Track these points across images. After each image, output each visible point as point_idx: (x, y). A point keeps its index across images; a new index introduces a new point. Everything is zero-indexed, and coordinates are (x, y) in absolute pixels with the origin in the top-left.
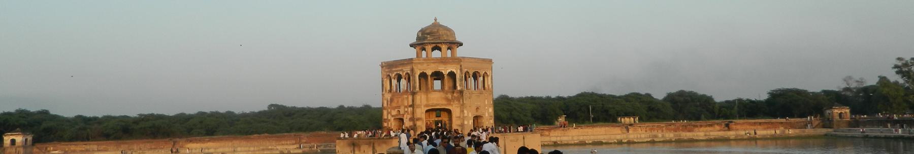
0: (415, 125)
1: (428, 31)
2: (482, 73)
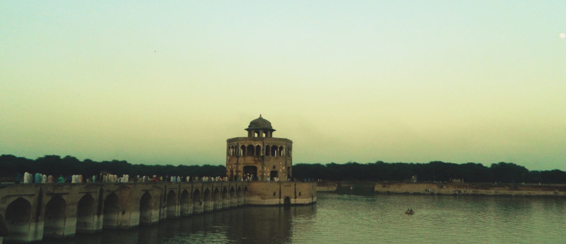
0: (237, 174)
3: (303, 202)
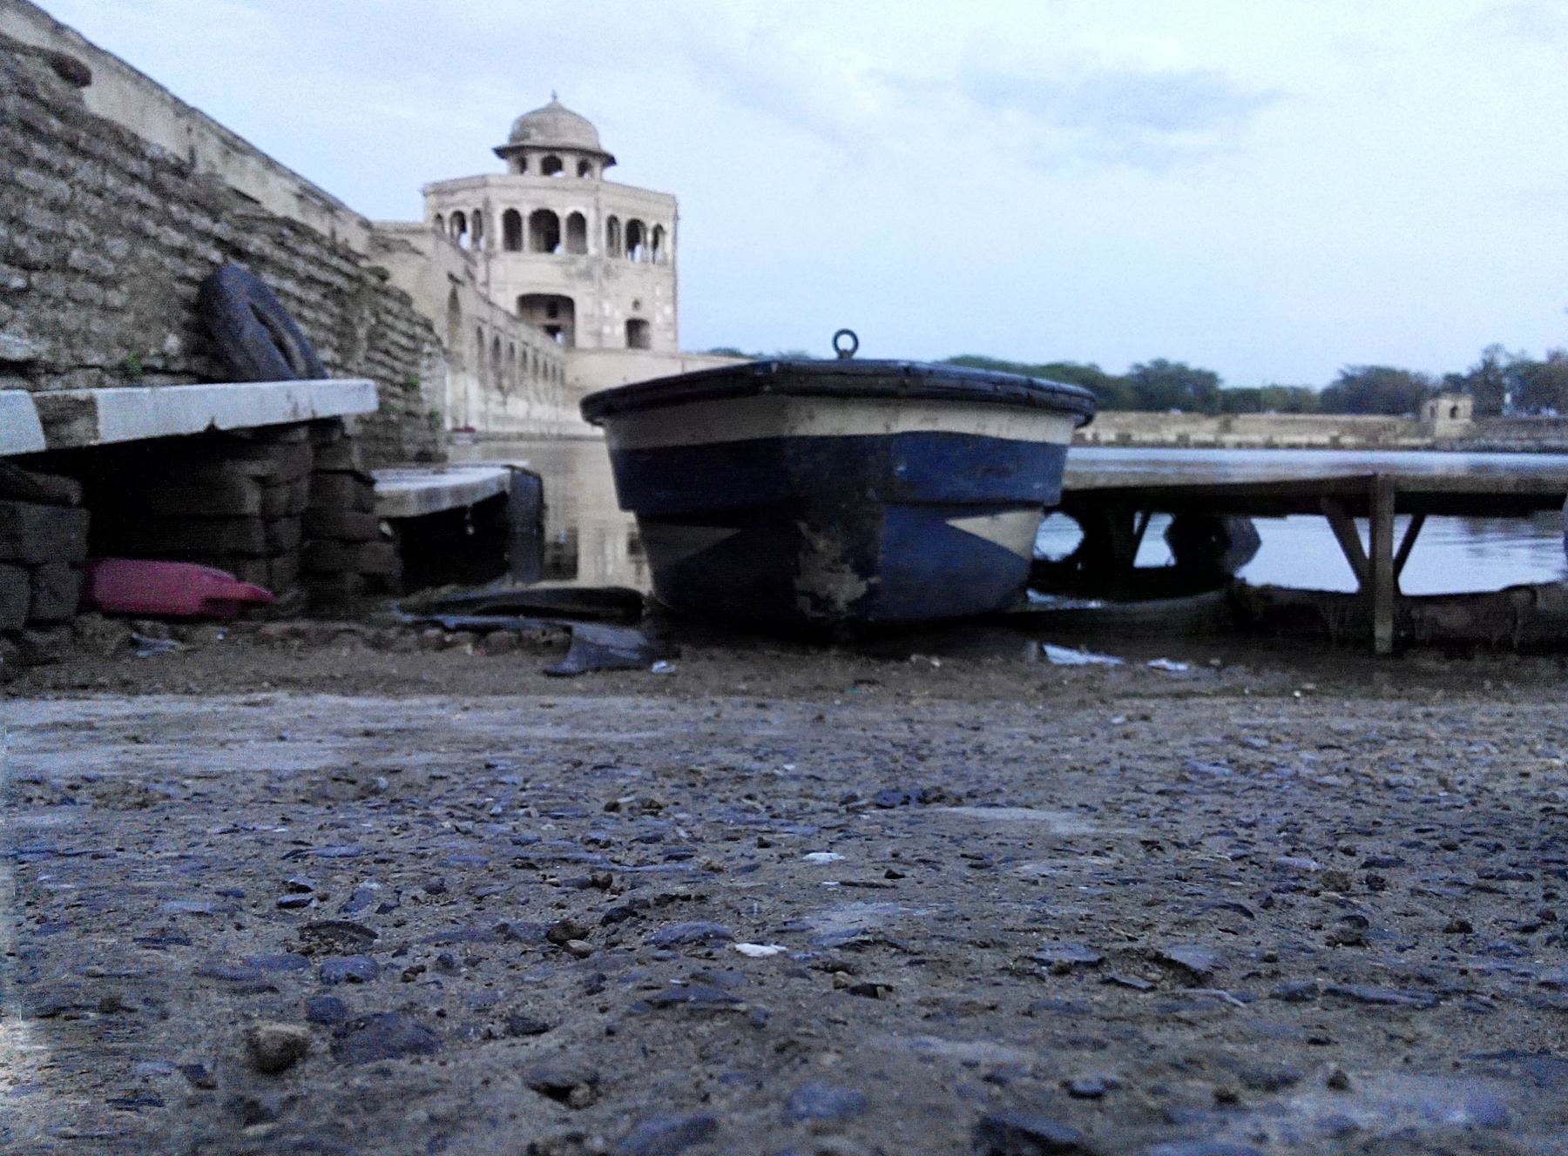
1: (534, 119)
2: (651, 224)
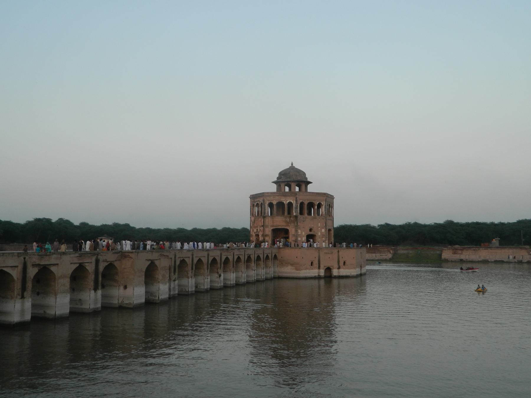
0: (264, 239)
1: (283, 173)
3: (348, 274)
